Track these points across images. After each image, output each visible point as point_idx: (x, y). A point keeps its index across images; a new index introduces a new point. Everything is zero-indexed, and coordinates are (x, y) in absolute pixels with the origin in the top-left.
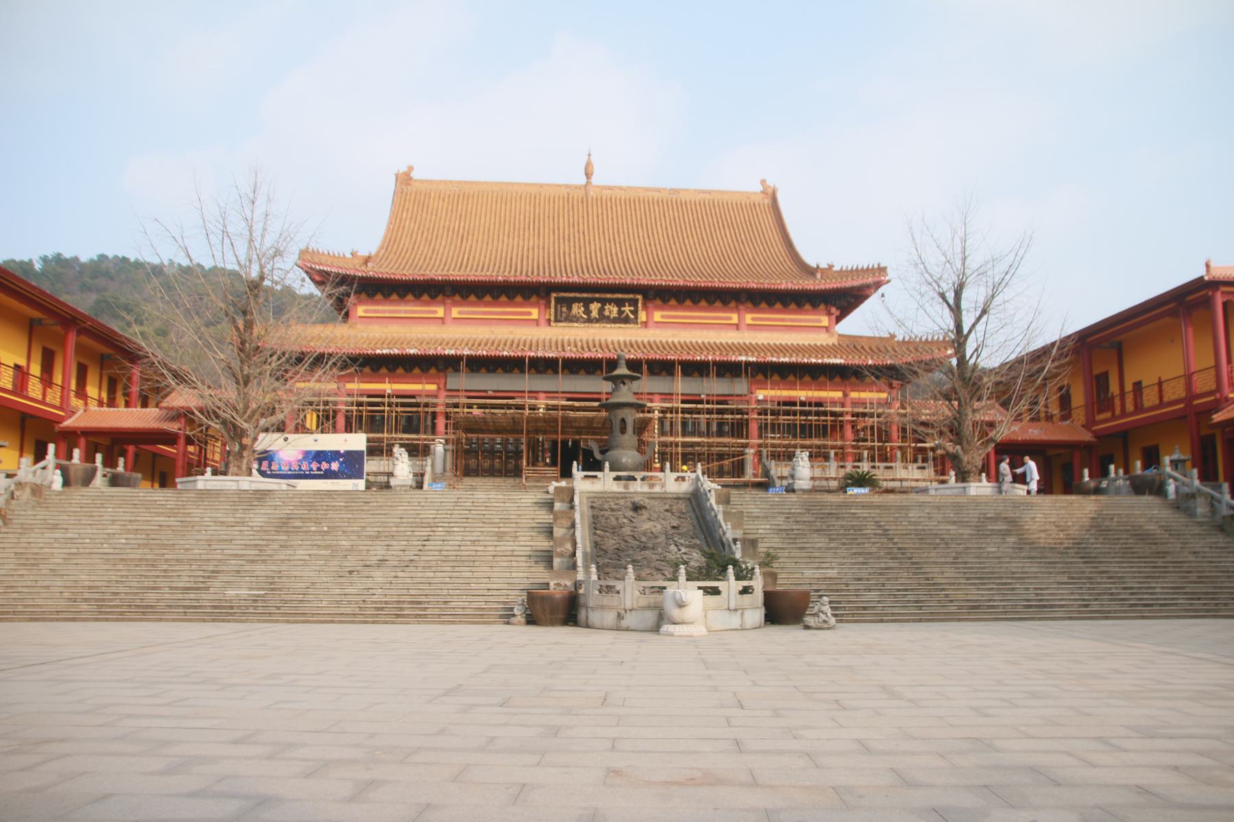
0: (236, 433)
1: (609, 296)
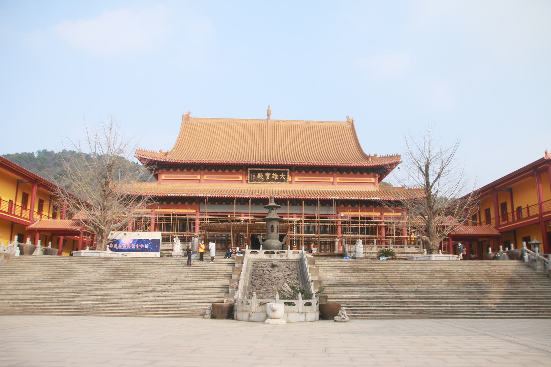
0: (101, 232)
1: (274, 170)
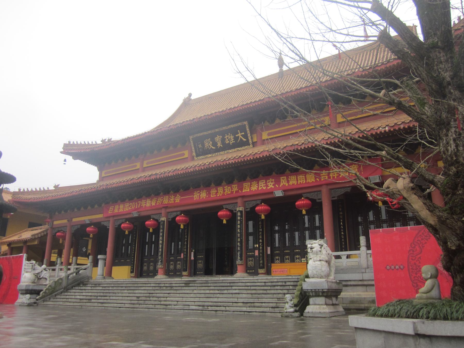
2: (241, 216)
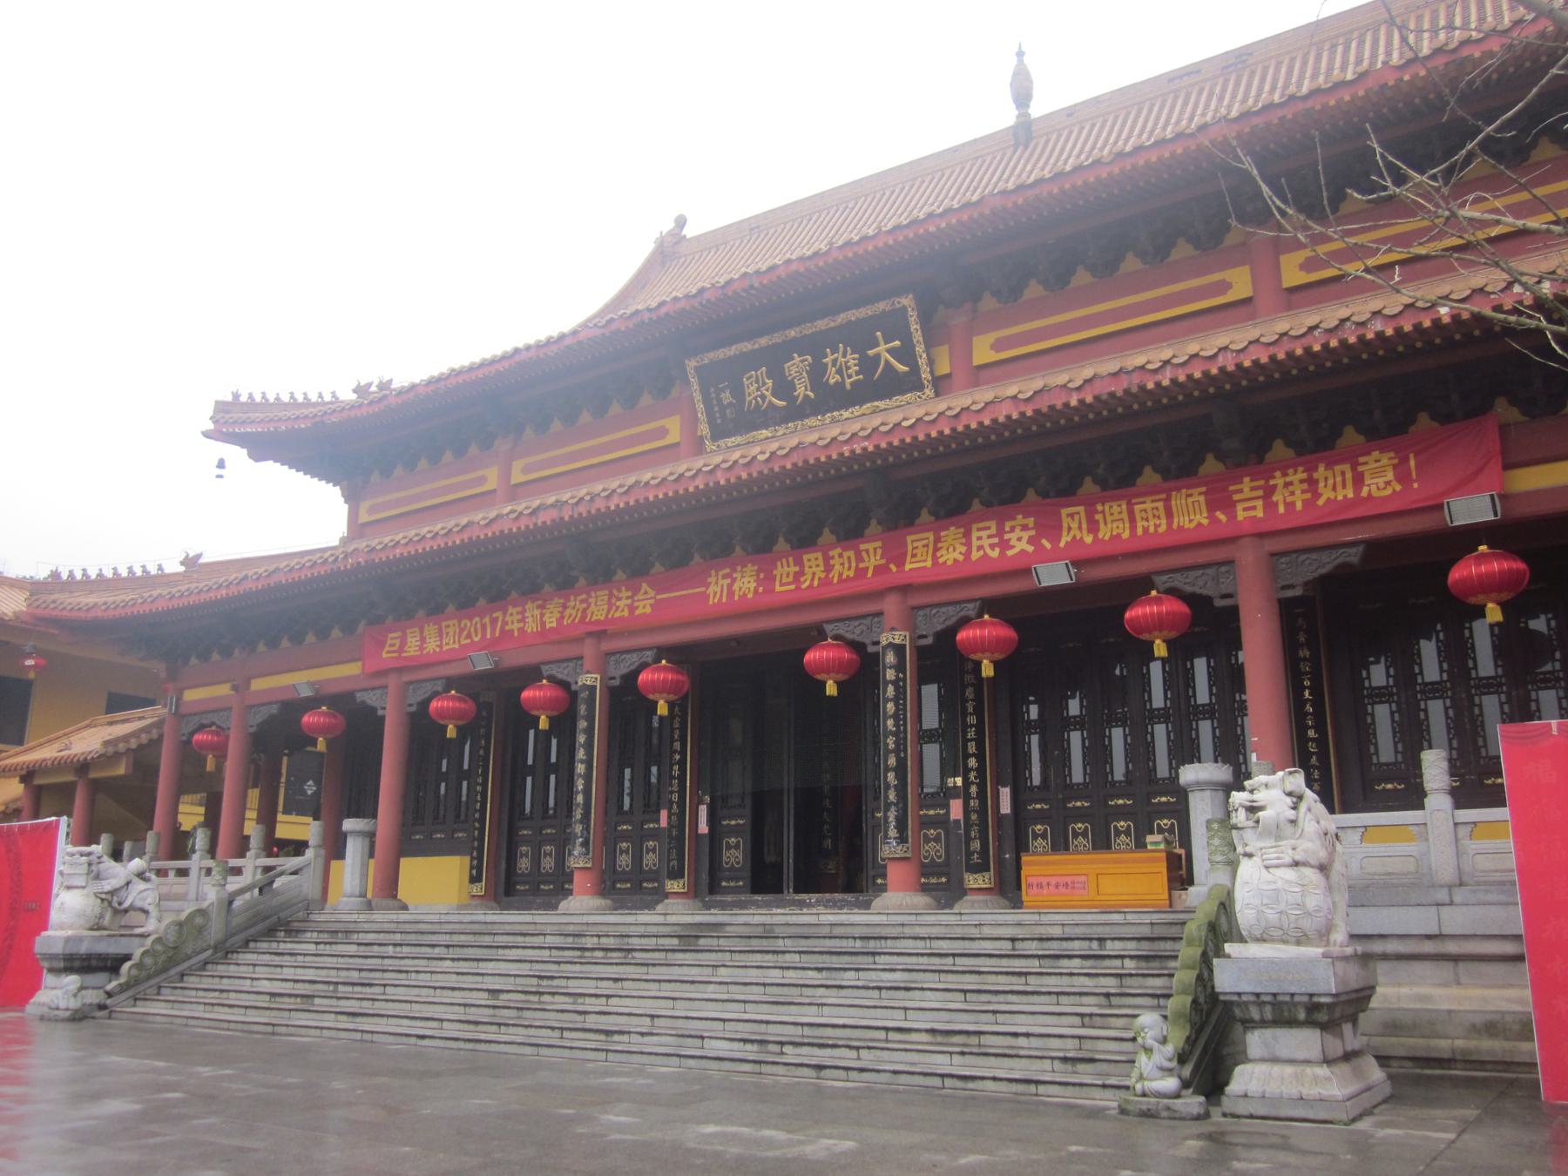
1: (821, 324)
2: (900, 667)
